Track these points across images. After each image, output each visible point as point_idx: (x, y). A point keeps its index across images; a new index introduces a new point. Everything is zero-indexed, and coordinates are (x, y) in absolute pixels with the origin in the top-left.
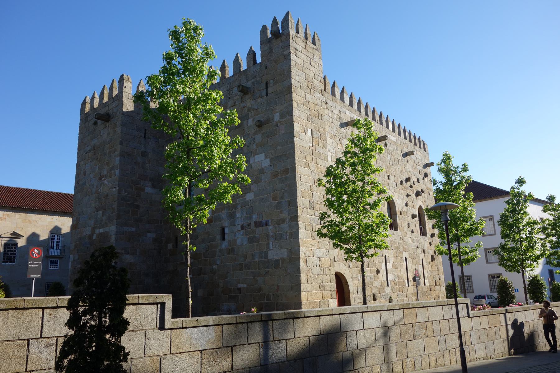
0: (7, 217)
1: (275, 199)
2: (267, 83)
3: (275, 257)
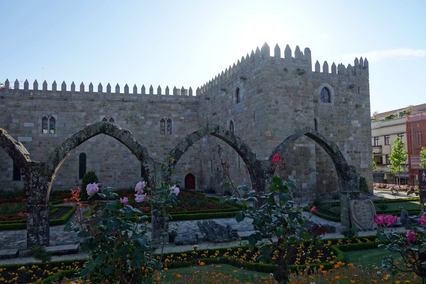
1: (363, 142)
3: (363, 167)
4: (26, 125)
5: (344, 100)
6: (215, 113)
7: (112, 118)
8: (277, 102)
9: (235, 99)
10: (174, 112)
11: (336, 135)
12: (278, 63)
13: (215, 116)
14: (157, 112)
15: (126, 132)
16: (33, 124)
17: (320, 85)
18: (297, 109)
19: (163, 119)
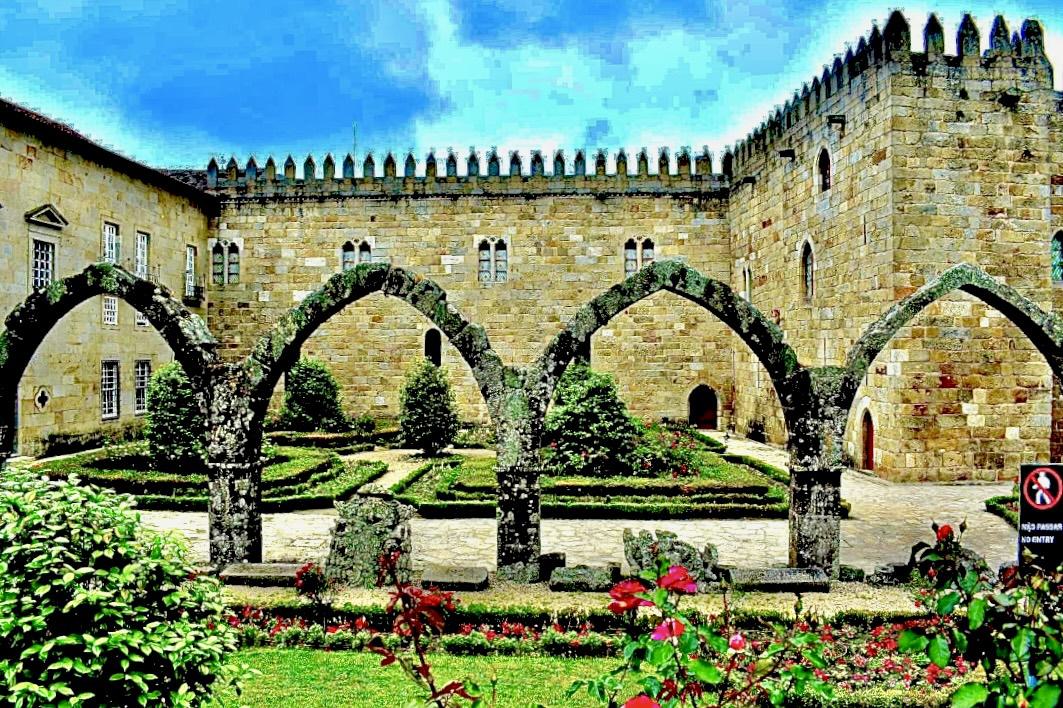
0: (33, 158)
4: (311, 262)
6: (767, 220)
7: (501, 242)
8: (931, 189)
9: (817, 179)
10: (661, 220)
12: (937, 72)
13: (768, 228)
14: (617, 222)
15: (432, 289)
16: (324, 259)
18: (997, 206)
19: (631, 241)
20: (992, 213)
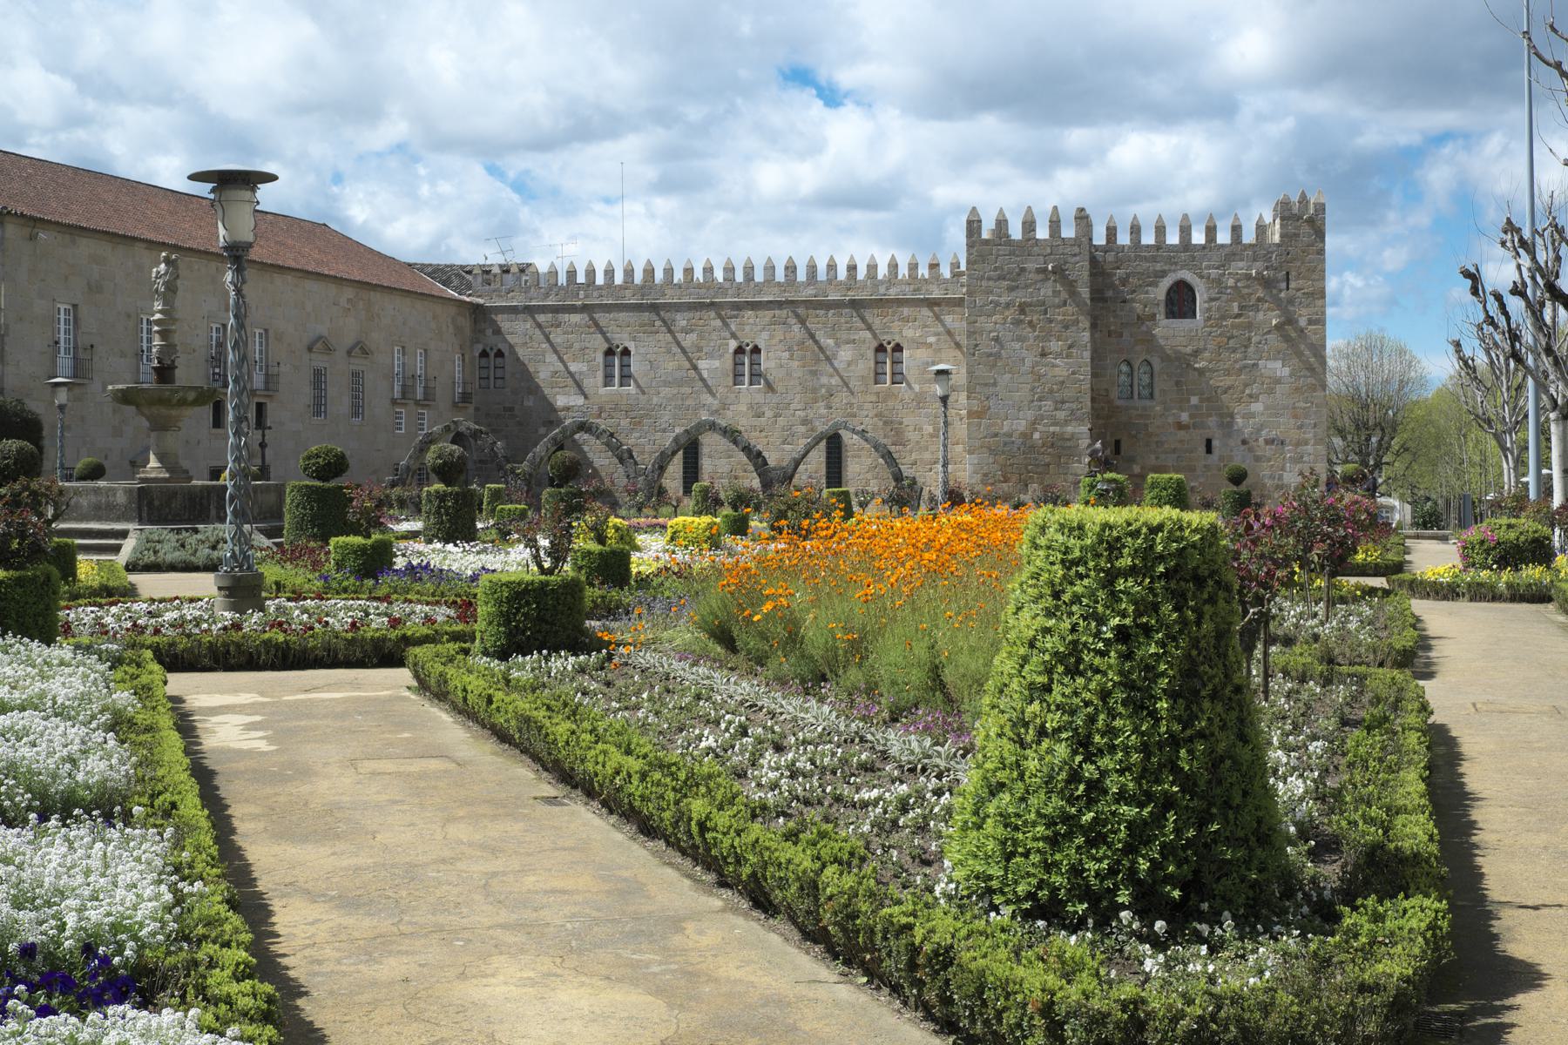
2: (1288, 273)
5: (1236, 310)
11: (1208, 400)
17: (1163, 274)
20: (1043, 355)
